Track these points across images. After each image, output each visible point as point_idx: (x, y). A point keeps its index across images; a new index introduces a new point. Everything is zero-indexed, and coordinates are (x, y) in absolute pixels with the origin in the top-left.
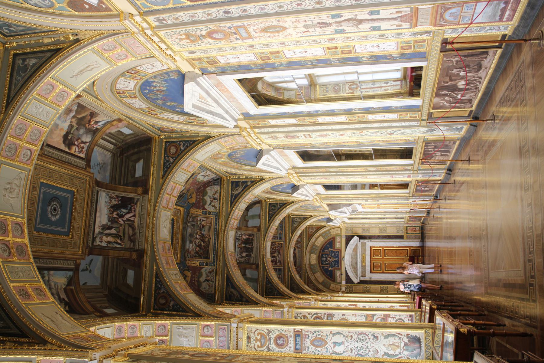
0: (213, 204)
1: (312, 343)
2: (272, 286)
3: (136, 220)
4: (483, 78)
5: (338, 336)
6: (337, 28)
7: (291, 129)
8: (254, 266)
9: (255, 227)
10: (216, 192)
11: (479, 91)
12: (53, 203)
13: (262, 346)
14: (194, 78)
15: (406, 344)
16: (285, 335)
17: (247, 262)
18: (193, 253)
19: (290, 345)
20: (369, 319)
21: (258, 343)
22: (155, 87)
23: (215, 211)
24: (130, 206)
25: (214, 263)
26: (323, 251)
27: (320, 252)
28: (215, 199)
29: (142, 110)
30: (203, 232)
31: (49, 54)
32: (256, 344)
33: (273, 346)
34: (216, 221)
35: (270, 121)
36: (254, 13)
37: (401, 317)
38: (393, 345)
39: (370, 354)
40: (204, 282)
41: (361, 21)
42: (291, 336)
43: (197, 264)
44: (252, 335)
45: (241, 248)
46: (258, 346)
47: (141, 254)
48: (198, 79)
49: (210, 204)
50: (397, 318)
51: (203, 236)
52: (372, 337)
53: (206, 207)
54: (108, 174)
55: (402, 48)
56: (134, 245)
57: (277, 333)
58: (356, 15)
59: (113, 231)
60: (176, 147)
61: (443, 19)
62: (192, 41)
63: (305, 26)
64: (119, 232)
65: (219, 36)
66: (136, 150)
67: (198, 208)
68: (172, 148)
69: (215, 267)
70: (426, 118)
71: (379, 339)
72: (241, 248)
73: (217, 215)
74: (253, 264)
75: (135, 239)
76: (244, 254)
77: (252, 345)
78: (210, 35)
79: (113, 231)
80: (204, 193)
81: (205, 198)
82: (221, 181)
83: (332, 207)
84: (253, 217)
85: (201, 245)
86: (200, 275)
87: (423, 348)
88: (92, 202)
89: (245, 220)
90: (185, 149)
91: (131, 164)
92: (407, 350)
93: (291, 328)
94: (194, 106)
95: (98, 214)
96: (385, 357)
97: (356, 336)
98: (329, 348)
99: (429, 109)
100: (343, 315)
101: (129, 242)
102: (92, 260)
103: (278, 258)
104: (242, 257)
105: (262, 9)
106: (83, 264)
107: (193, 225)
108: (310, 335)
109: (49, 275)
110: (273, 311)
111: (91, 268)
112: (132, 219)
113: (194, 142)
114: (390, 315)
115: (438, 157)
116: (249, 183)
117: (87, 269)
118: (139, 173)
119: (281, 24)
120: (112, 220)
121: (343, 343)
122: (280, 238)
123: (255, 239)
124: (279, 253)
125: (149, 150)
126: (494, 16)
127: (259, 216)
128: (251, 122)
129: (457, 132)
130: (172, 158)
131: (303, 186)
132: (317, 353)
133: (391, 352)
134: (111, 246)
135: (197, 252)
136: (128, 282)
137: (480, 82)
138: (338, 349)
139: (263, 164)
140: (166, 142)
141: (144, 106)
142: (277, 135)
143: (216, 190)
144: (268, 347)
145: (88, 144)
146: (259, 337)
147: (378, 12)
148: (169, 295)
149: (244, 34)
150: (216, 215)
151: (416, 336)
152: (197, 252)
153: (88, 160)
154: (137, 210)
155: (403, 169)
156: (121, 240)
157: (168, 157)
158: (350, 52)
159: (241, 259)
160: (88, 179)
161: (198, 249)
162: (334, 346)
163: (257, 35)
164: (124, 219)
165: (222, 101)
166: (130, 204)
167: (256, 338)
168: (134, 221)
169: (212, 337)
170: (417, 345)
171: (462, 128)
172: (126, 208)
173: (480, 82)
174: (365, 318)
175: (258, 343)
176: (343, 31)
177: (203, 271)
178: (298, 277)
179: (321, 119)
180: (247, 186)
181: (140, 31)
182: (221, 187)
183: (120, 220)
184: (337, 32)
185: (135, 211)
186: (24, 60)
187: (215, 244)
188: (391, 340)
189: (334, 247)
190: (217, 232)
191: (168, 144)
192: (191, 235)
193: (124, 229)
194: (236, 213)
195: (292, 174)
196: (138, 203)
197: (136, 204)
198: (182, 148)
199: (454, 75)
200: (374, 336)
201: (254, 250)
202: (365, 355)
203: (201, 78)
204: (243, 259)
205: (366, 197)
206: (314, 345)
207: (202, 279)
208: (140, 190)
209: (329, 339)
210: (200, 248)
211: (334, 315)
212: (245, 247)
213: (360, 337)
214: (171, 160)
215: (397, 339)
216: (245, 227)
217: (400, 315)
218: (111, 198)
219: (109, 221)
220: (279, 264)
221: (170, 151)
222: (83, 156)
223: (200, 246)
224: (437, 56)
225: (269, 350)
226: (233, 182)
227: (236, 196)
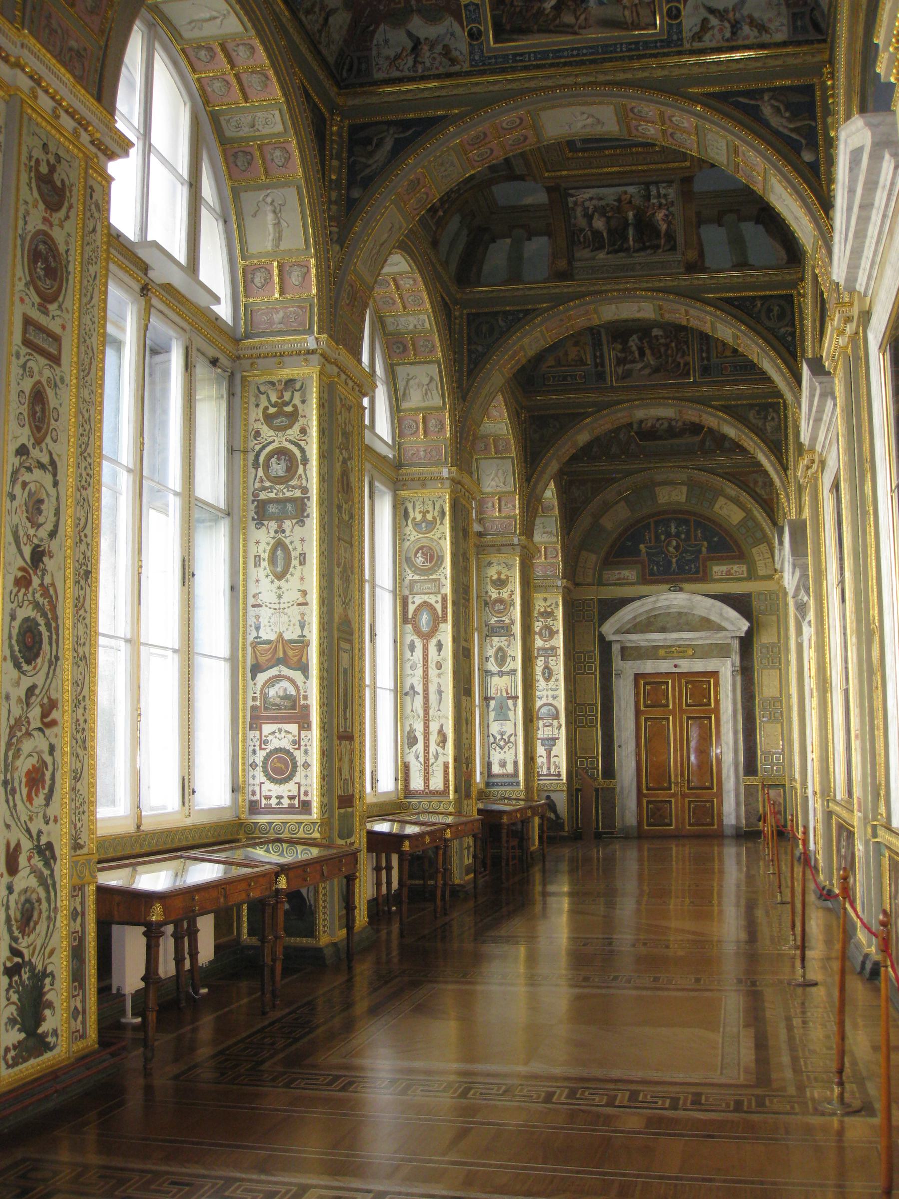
0: (714, 21)
8: (563, 264)
9: (701, 255)
10: (762, 28)
20: (290, 653)
23: (686, 34)
26: (698, 524)
27: (695, 514)
28: (735, 27)
34: (646, 45)
37: (300, 769)
40: (409, 35)
45: (619, 210)
50: (299, 756)
69: (466, 67)
72: (619, 210)
74: (571, 260)
76: (599, 224)
82: (811, 42)
84: (737, 242)
86: (431, 16)
103: (639, 366)
104: (589, 218)
110: (309, 299)
114: (309, 728)
116: (807, 157)
124: (657, 370)
127: (742, 264)
150: (668, 43)
159: (579, 212)
174: (295, 637)
177: (449, 22)
178: (583, 438)
180: (796, 148)
182: (784, 44)
189: (712, 559)
190: (603, 54)
201: (620, 259)
204: (582, 222)
207: (418, 26)
211: (301, 522)
212: (626, 224)
216: (698, 214)
217: (306, 766)
220: (620, 370)
226: (809, 90)
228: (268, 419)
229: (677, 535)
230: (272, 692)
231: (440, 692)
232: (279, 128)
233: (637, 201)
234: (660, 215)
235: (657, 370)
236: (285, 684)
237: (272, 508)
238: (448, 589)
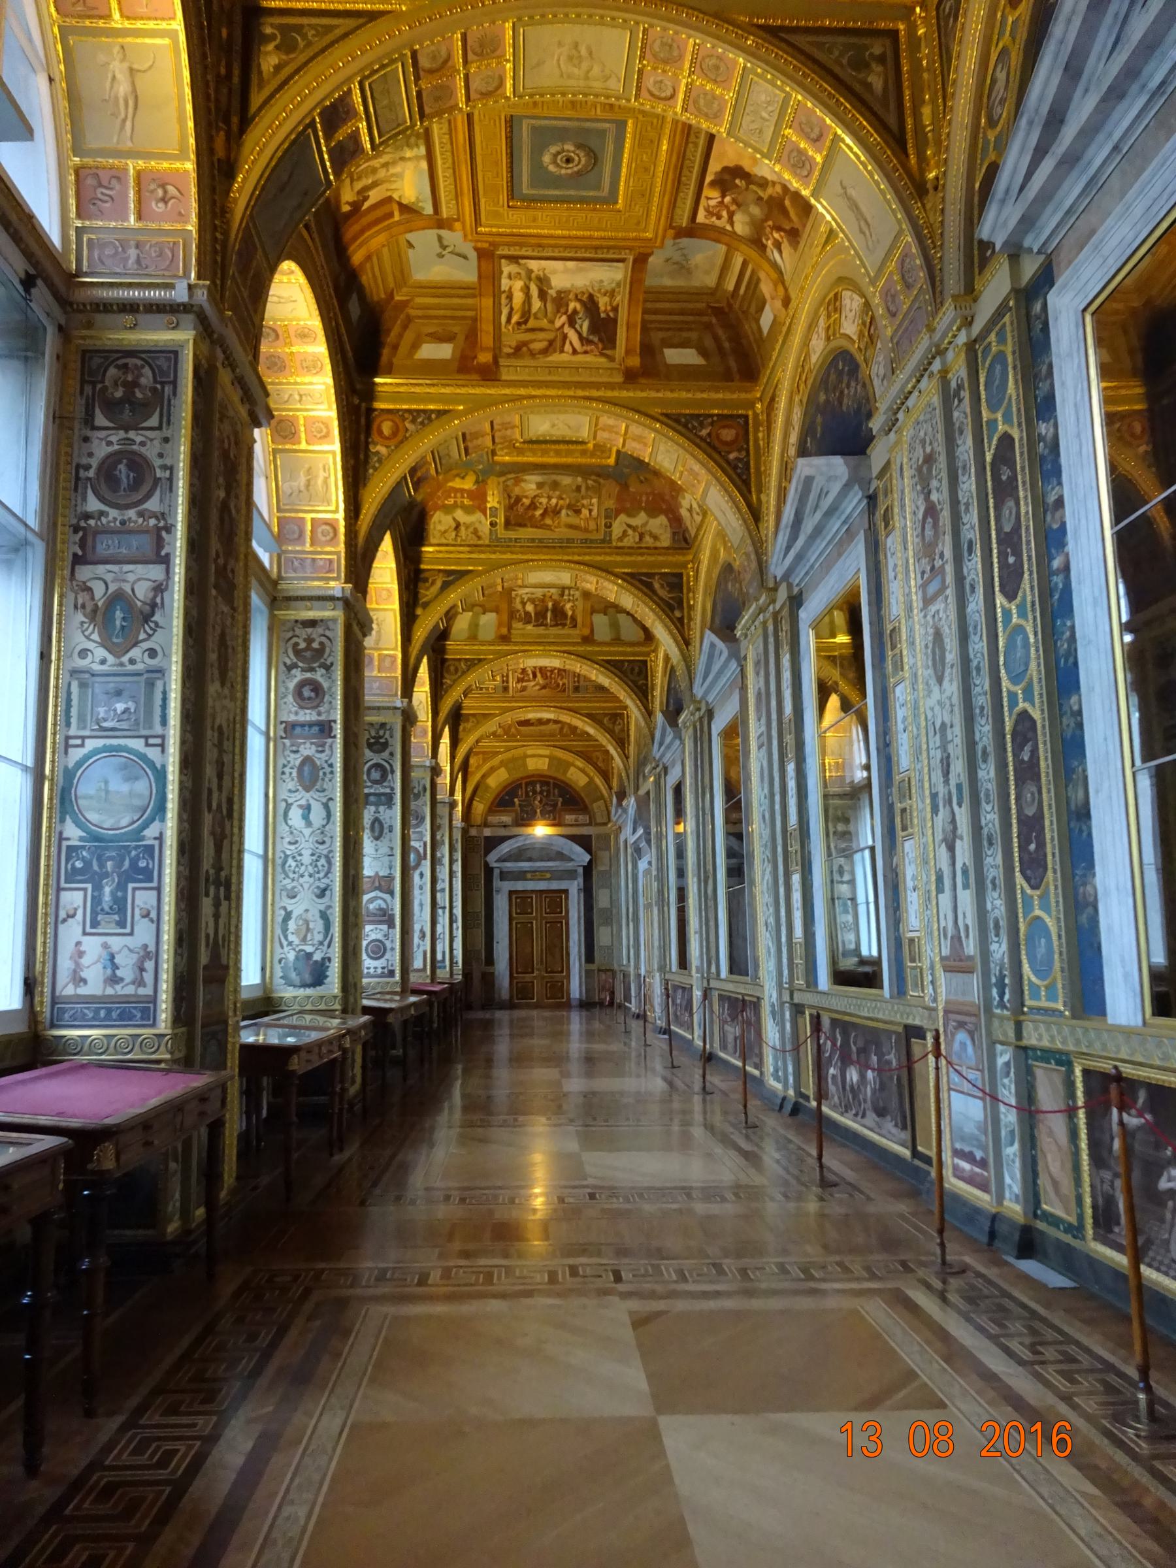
0: (630, 532)
1: (307, 760)
2: (464, 673)
3: (565, 357)
4: (865, 1121)
5: (324, 814)
6: (941, 795)
7: (774, 703)
8: (504, 631)
9: (592, 631)
11: (842, 1114)
12: (582, 154)
13: (297, 652)
14: (857, 478)
15: (309, 956)
16: (322, 701)
17: (512, 614)
18: (517, 491)
19: (301, 712)
21: (303, 645)
22: (848, 386)
23: (615, 536)
24: (596, 339)
25: (498, 540)
28: (641, 536)
29: (808, 355)
30: (564, 512)
31: (892, 121)
32: (300, 641)
33: (298, 676)
34: (592, 541)
35: (788, 656)
36: (969, 610)
38: (308, 929)
39: (288, 881)
41: (951, 849)
42: (319, 714)
43: (492, 501)
44: (320, 630)
46: (297, 644)
47: (489, 374)
48: (856, 487)
49: (629, 526)
50: (388, 944)
51: (556, 512)
53: (623, 518)
54: (668, 282)
55: (912, 940)
56: (509, 355)
57: (325, 685)
58: (961, 838)
59: (537, 304)
60: (733, 442)
61: (956, 1028)
62: (919, 470)
63: (943, 724)
64: (536, 318)
65: (929, 532)
66: (727, 345)
67: (620, 499)
68: (733, 432)
70: (796, 1001)
72: (543, 601)
73: (607, 540)
74: (510, 628)
75: (522, 357)
76: (530, 608)
77: (298, 631)
78: (931, 511)
79: (537, 304)
80: (653, 512)
81: (643, 514)
83: (643, 803)
84: (615, 626)
85: (536, 508)
86: (468, 510)
87: (301, 992)
88: (596, 248)
89: (606, 607)
90: (728, 462)
91: (694, 335)
92: (297, 958)
93: (338, 716)
94: (809, 481)
95: (570, 264)
96: (283, 913)
98: (298, 795)
99: (811, 1007)
100: (391, 829)
101: (514, 344)
102: (465, 258)
104: (524, 604)
105: (975, 627)
106: (453, 238)
107: (578, 489)
108: (323, 756)
109: (417, 158)
111: (448, 256)
112: (567, 347)
113: (747, 483)
115: (733, 1031)
117: (444, 247)
118: (674, 356)
119: (948, 671)
120: (561, 300)
121: (309, 824)
122: (577, 689)
123: (566, 631)
124: (544, 687)
125: (727, 376)
126: (963, 1139)
128: (785, 612)
129: (772, 1069)
130: (709, 435)
131: (678, 736)
132: (287, 770)
133: (292, 925)
134: (504, 301)
135: (518, 500)
136: (425, 346)
137: (856, 1115)
138: (295, 815)
139: (713, 645)
140: (746, 417)
141: (814, 358)
142: (762, 673)
143: (662, 538)
144: (295, 666)
145: (728, 228)
146: (315, 645)
147: (966, 886)
148: (402, 442)
149: (932, 589)
150: (603, 541)
152: (518, 500)
153: (693, 230)
154: (588, 358)
155: (710, 955)
156: (519, 324)
157: (712, 424)
158: (904, 829)
160: (649, 235)
161: (527, 502)
162: (300, 806)
163: (929, 618)
164: (567, 329)
165: (820, 544)
166: (600, 340)
167: (313, 640)
168: (562, 351)
169: (312, 545)
170: (308, 978)
171: (777, 1079)
172: (593, 329)
173: (856, 1115)
175: (303, 645)
176: (935, 810)
177: (478, 515)
179: (791, 768)
180: (672, 609)
181: (937, 346)
183: (564, 318)
184: (934, 796)
185: (586, 352)
186: (881, 59)
187: (541, 540)
188: (318, 925)
191: (741, 421)
192: (555, 485)
193: (542, 330)
194: (610, 586)
195: (699, 709)
196: (603, 360)
197: (602, 355)
198: (732, 456)
199: (868, 1058)
200: (325, 890)
201: (541, 630)
202: (284, 872)
203: (860, 494)
204: (519, 607)
205: (661, 878)
206: (303, 763)
207: (460, 515)
208: (635, 361)
209: (317, 795)
210: (529, 507)
213: (323, 861)
214: (704, 432)
215: (320, 937)
217: (393, 949)
218: (612, 294)
219: (559, 292)
221: (724, 427)
222: (701, 217)
223: (533, 506)
224: (898, 1019)
225: (289, 668)
226: (680, 575)
227: (649, 586)
228: (370, 746)
229: (541, 792)
230: (371, 906)
231: (421, 905)
232: (388, 579)
233: (555, 597)
234: (568, 606)
235: (544, 687)
236: (379, 901)
237: (372, 798)
238: (428, 839)
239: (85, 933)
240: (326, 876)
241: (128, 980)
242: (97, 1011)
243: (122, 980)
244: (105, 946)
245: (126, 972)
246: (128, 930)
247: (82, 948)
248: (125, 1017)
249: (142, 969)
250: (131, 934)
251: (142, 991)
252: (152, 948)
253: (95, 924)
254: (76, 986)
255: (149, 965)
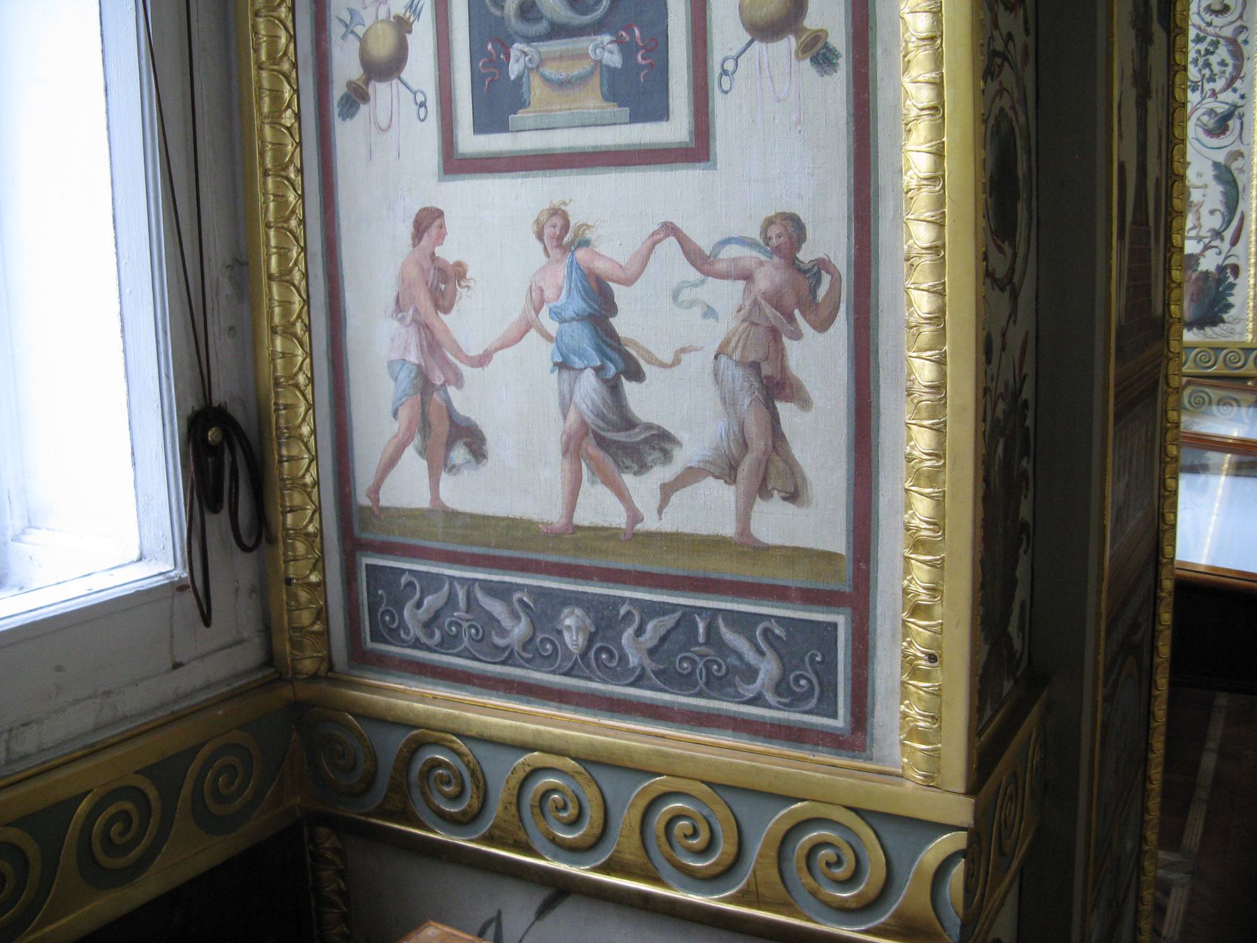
52: (1221, 109)
71: (1215, 142)
97: (1228, 32)
151: (1230, 306)
213: (1223, 52)
215: (1216, 222)
239: (455, 164)
240: (1230, 84)
241: (690, 451)
242: (544, 610)
243: (662, 441)
244: (560, 234)
245: (685, 401)
246: (675, 129)
247: (448, 252)
248: (690, 665)
249: (775, 386)
250: (698, 150)
251: (776, 523)
252: (829, 240)
253: (497, 104)
254: (438, 465)
255: (819, 358)
